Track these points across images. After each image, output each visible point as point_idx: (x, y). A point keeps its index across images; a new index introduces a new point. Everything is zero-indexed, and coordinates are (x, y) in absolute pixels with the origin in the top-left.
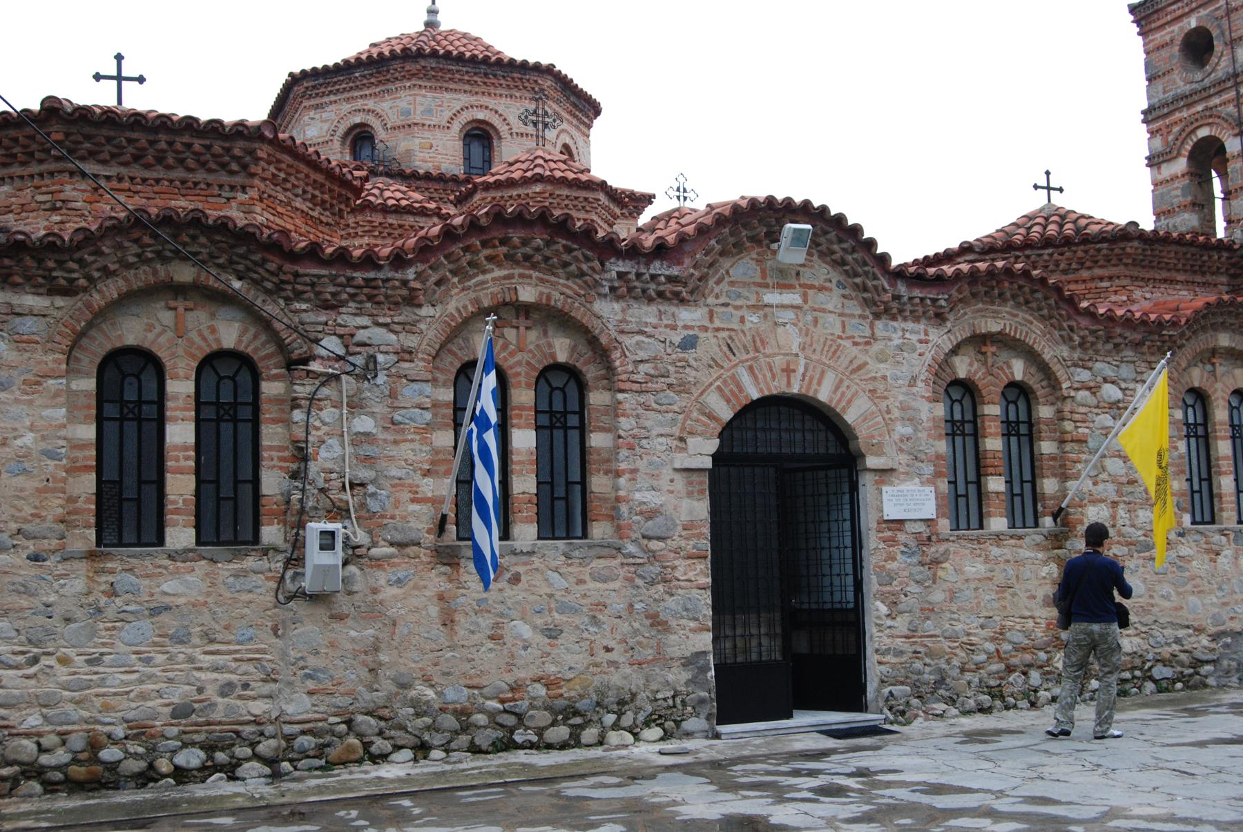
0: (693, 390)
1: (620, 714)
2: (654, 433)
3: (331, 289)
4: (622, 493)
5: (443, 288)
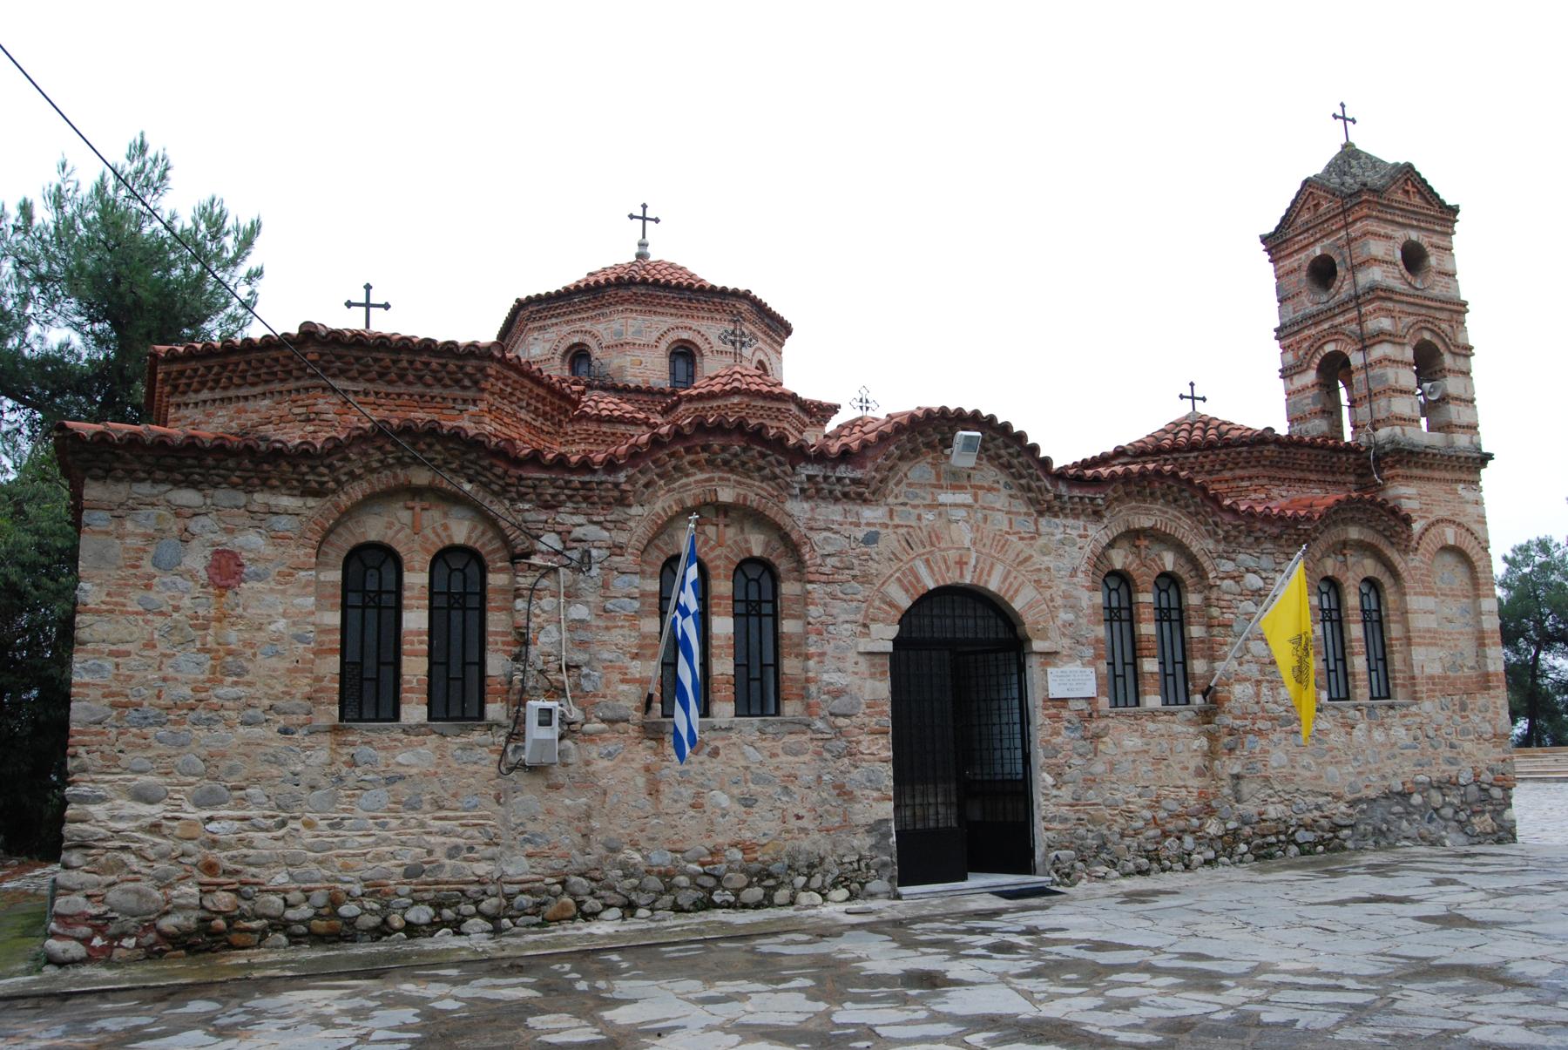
0: (875, 581)
1: (810, 877)
2: (840, 619)
3: (551, 491)
4: (811, 674)
5: (651, 490)
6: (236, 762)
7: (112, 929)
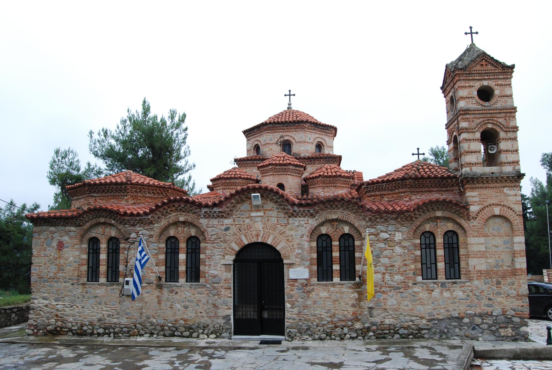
1: (204, 330)
3: (132, 222)
6: (62, 291)
7: (38, 328)
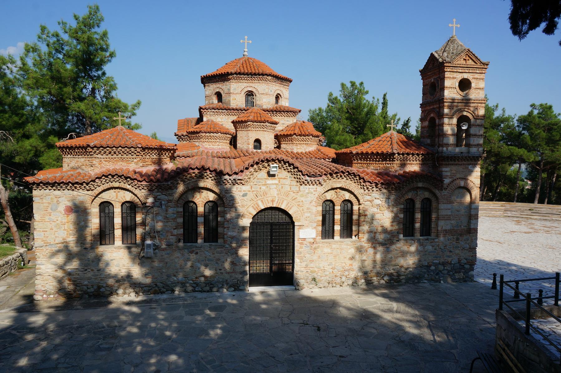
4: (225, 233)
